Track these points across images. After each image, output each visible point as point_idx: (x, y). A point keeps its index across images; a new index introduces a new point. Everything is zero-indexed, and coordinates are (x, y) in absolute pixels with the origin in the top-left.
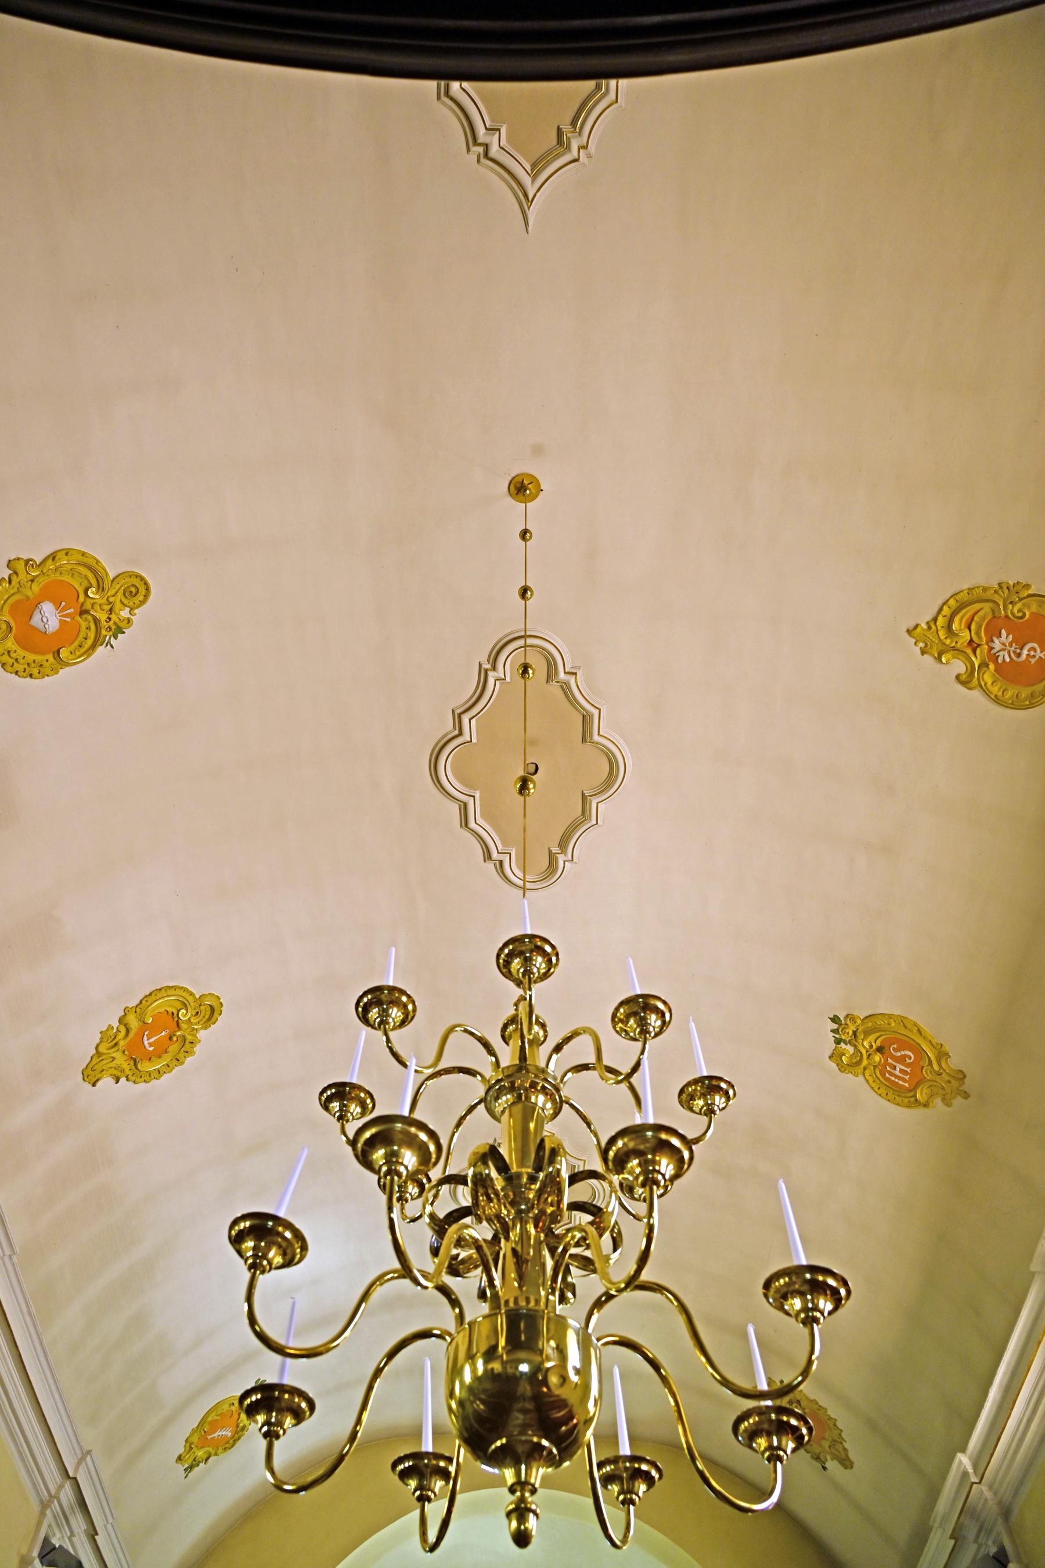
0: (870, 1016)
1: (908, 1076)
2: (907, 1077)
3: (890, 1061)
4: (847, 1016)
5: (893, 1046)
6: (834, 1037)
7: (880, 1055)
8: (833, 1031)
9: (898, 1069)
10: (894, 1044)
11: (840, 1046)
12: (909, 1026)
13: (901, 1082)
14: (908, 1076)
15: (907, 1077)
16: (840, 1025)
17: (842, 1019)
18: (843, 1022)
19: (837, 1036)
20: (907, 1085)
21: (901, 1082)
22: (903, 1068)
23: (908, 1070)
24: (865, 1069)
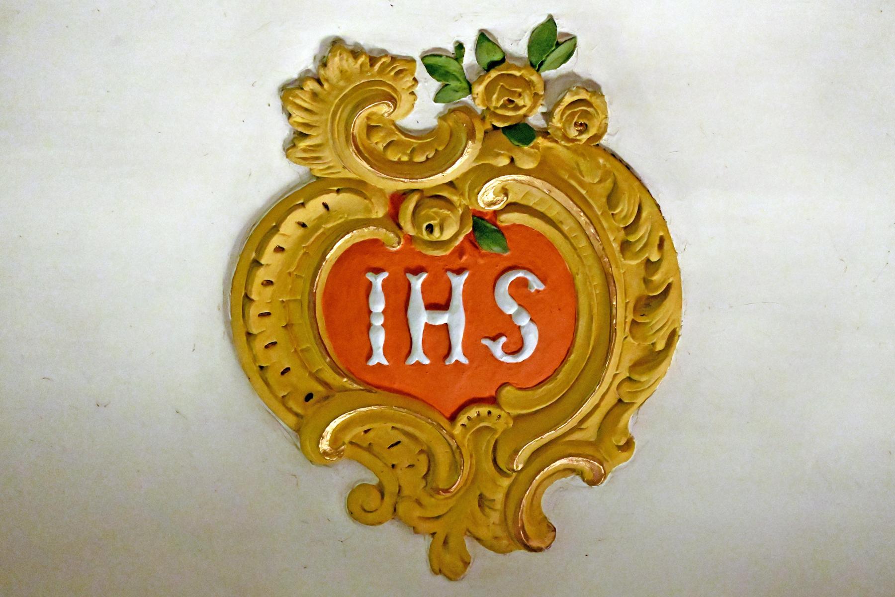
0: (628, 167)
1: (426, 361)
2: (419, 356)
3: (459, 282)
4: (594, 88)
5: (530, 277)
6: (460, 47)
7: (461, 238)
8: (484, 37)
9: (442, 319)
10: (543, 281)
11: (420, 71)
12: (660, 317)
13: (379, 339)
14: (426, 361)
15: (419, 356)
16: (537, 66)
17: (565, 68)
18: (549, 73)
19: (469, 58)
20: (379, 358)
21: (379, 339)
22: (458, 336)
23: (458, 355)
24: (357, 187)
